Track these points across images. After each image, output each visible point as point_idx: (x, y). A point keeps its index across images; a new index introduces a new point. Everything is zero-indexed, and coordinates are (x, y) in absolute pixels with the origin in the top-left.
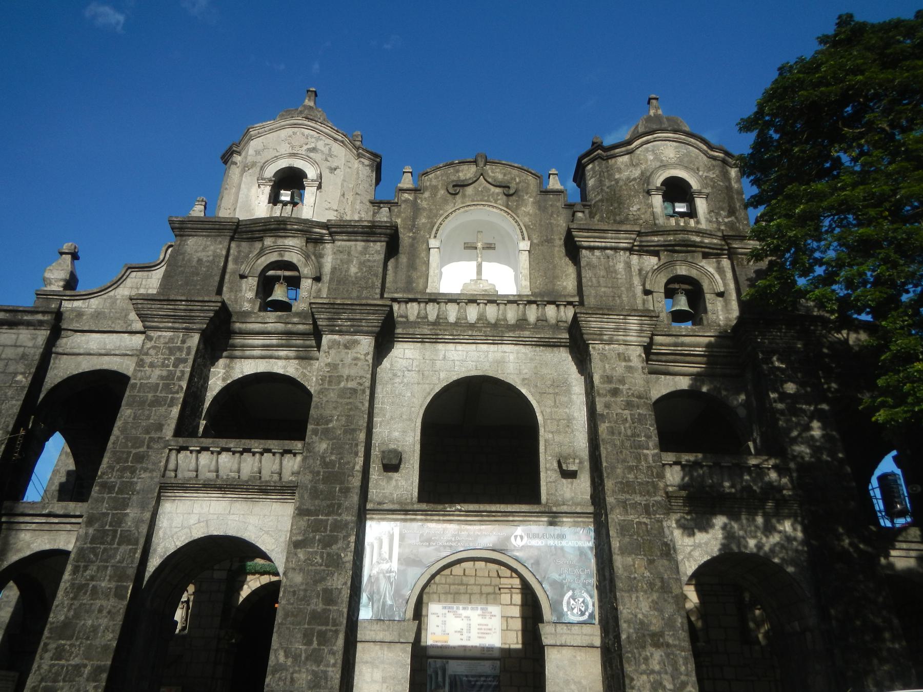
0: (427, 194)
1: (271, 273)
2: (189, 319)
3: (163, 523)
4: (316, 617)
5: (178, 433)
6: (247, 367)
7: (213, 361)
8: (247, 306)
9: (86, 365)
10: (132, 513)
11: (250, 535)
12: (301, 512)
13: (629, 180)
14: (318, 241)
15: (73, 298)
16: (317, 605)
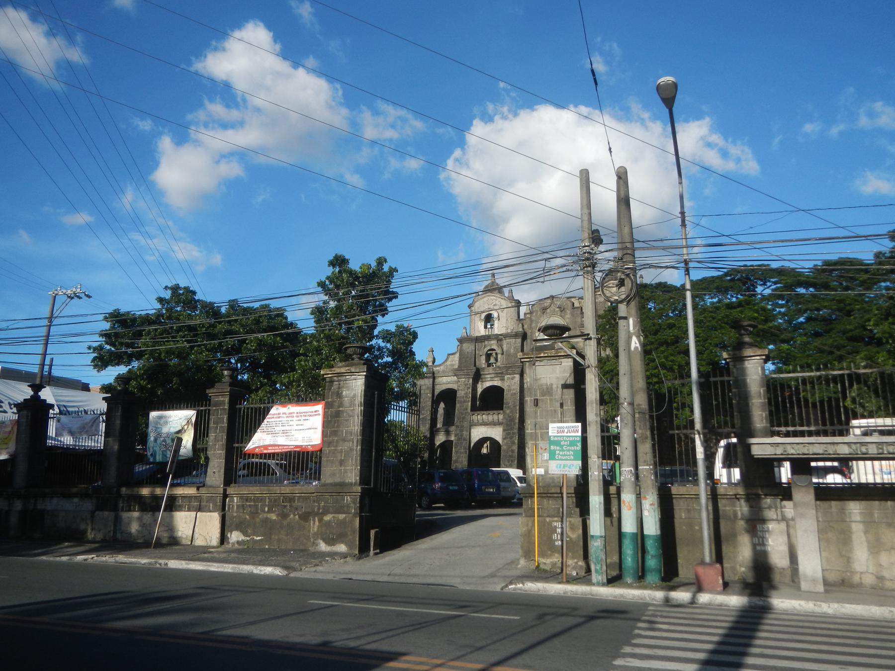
0: (534, 314)
1: (489, 352)
2: (467, 375)
3: (472, 434)
4: (511, 456)
5: (472, 410)
6: (488, 384)
7: (478, 383)
8: (484, 366)
9: (444, 387)
10: (465, 433)
11: (493, 436)
12: (504, 430)
13: (600, 302)
14: (501, 340)
15: (436, 366)
16: (510, 453)
